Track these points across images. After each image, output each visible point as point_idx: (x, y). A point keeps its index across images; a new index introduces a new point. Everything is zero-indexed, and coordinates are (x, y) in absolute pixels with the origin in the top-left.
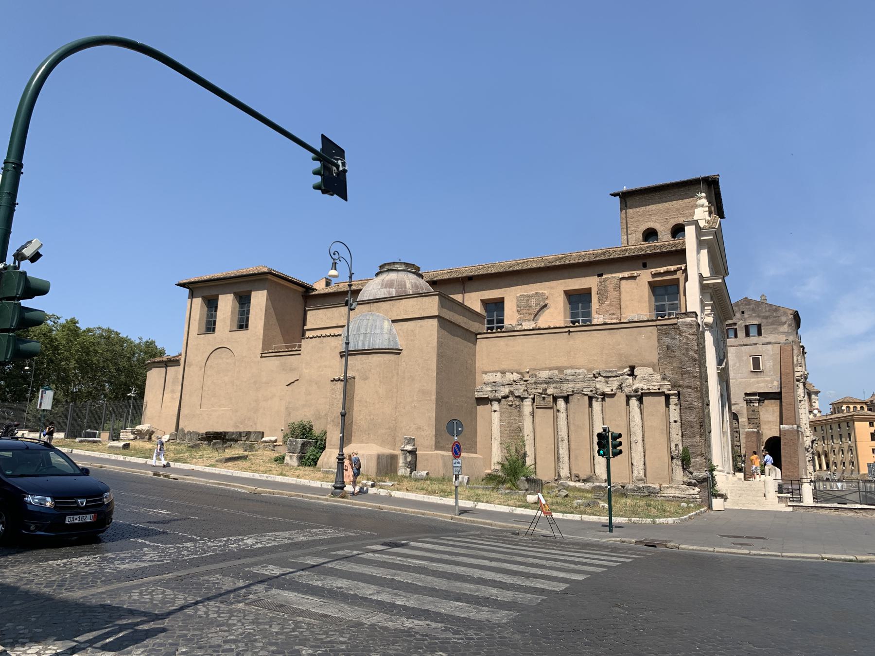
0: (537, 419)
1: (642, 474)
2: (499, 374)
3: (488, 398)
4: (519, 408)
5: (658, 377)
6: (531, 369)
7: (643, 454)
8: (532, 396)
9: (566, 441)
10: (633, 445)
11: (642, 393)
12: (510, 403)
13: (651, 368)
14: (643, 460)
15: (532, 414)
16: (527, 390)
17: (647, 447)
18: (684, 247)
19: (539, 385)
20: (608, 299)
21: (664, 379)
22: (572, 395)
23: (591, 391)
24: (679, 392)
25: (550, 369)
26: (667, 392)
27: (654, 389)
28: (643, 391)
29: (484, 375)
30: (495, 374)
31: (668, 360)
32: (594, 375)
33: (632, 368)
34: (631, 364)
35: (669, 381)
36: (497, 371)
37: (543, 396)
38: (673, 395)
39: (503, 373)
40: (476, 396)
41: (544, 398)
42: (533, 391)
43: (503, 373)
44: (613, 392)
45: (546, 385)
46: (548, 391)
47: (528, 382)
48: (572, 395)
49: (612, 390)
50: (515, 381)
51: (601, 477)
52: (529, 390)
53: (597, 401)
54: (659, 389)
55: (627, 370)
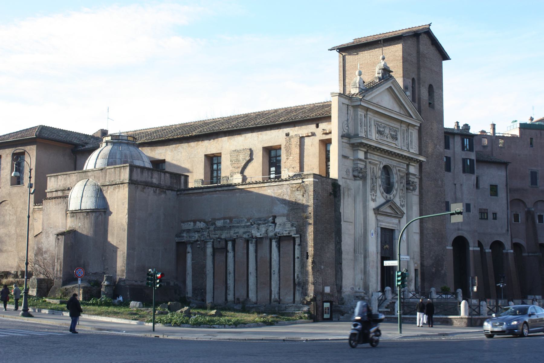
0: (216, 258)
1: (277, 297)
2: (192, 224)
3: (184, 242)
4: (204, 249)
5: (288, 225)
6: (212, 219)
7: (278, 282)
8: (212, 240)
9: (232, 274)
10: (272, 275)
11: (280, 237)
12: (198, 246)
13: (285, 218)
14: (278, 286)
15: (214, 255)
16: (209, 236)
17: (281, 277)
18: (330, 115)
19: (216, 232)
20: (292, 155)
21: (292, 225)
22: (237, 238)
23: (248, 235)
24: (301, 235)
25: (224, 219)
26: (293, 236)
27: (285, 233)
28: (279, 235)
29: (182, 224)
30: (189, 223)
31: (295, 211)
32: (251, 223)
33: (274, 217)
34: (273, 214)
35: (295, 227)
36: (191, 221)
37: (218, 240)
38: (297, 237)
39: (195, 222)
40: (177, 241)
41: (219, 241)
42: (213, 236)
43: (195, 222)
44: (261, 236)
45: (221, 232)
46: (222, 236)
47: (210, 229)
48: (237, 238)
49: (261, 235)
50: (202, 229)
51: (252, 300)
52: (211, 236)
53: (251, 243)
54: (289, 233)
55: (271, 219)
